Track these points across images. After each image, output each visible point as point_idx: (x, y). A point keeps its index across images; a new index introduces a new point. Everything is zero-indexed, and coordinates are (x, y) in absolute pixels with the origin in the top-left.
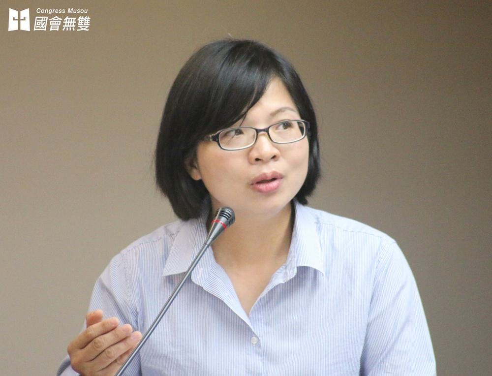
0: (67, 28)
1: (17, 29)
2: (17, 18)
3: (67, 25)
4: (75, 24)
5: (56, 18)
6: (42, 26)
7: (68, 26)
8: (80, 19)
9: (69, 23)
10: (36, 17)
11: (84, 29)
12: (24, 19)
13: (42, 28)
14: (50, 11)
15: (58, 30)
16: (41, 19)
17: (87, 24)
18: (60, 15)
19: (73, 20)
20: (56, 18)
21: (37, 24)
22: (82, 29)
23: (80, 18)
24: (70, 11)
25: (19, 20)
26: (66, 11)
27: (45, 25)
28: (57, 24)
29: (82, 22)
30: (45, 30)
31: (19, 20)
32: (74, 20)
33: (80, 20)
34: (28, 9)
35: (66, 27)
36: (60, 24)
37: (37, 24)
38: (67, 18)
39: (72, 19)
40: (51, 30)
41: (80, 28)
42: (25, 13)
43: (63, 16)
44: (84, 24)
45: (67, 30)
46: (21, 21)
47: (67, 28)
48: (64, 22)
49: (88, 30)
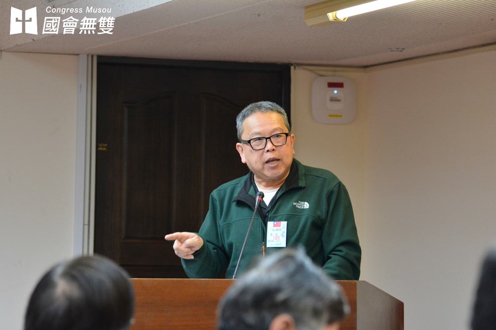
0: (85, 31)
1: (21, 32)
2: (20, 18)
3: (85, 27)
4: (95, 26)
5: (71, 19)
6: (53, 29)
7: (87, 28)
8: (102, 20)
9: (88, 25)
10: (46, 18)
11: (107, 32)
12: (30, 20)
13: (53, 31)
14: (63, 11)
15: (73, 33)
16: (51, 20)
17: (111, 26)
18: (75, 15)
19: (92, 21)
20: (71, 19)
21: (47, 26)
22: (105, 32)
23: (102, 18)
24: (89, 10)
25: (23, 22)
26: (84, 10)
27: (56, 27)
28: (72, 26)
29: (104, 24)
30: (57, 33)
31: (24, 21)
32: (94, 21)
33: (101, 22)
34: (34, 10)
35: (84, 30)
36: (75, 26)
37: (47, 26)
38: (85, 19)
39: (91, 19)
40: (64, 33)
41: (101, 31)
42: (32, 13)
43: (79, 16)
44: (106, 25)
45: (85, 33)
46: (26, 22)
47: (85, 31)
48: (81, 24)
49: (111, 33)
